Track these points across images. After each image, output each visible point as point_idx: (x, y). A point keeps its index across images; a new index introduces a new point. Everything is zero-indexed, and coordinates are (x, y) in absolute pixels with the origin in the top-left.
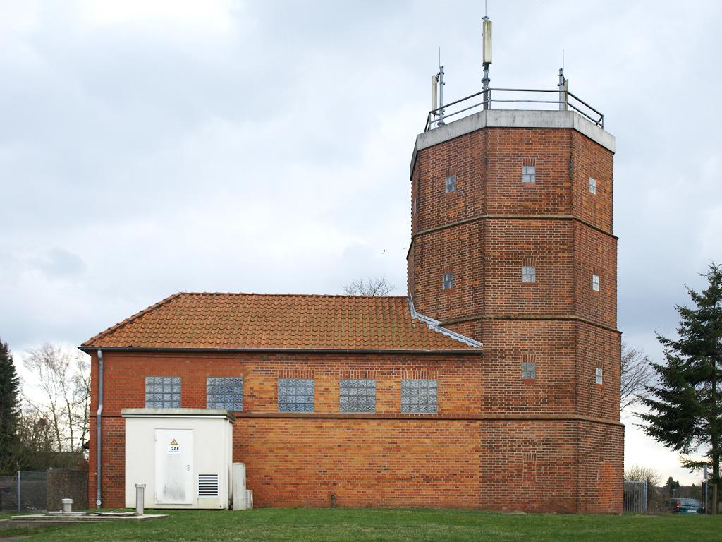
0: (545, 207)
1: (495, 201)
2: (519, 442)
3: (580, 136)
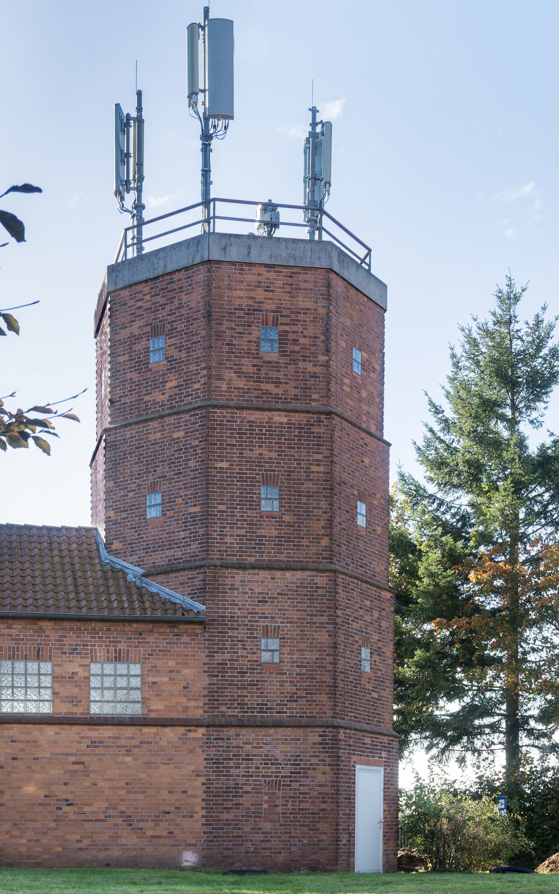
0: (293, 392)
1: (223, 379)
2: (257, 761)
3: (340, 283)
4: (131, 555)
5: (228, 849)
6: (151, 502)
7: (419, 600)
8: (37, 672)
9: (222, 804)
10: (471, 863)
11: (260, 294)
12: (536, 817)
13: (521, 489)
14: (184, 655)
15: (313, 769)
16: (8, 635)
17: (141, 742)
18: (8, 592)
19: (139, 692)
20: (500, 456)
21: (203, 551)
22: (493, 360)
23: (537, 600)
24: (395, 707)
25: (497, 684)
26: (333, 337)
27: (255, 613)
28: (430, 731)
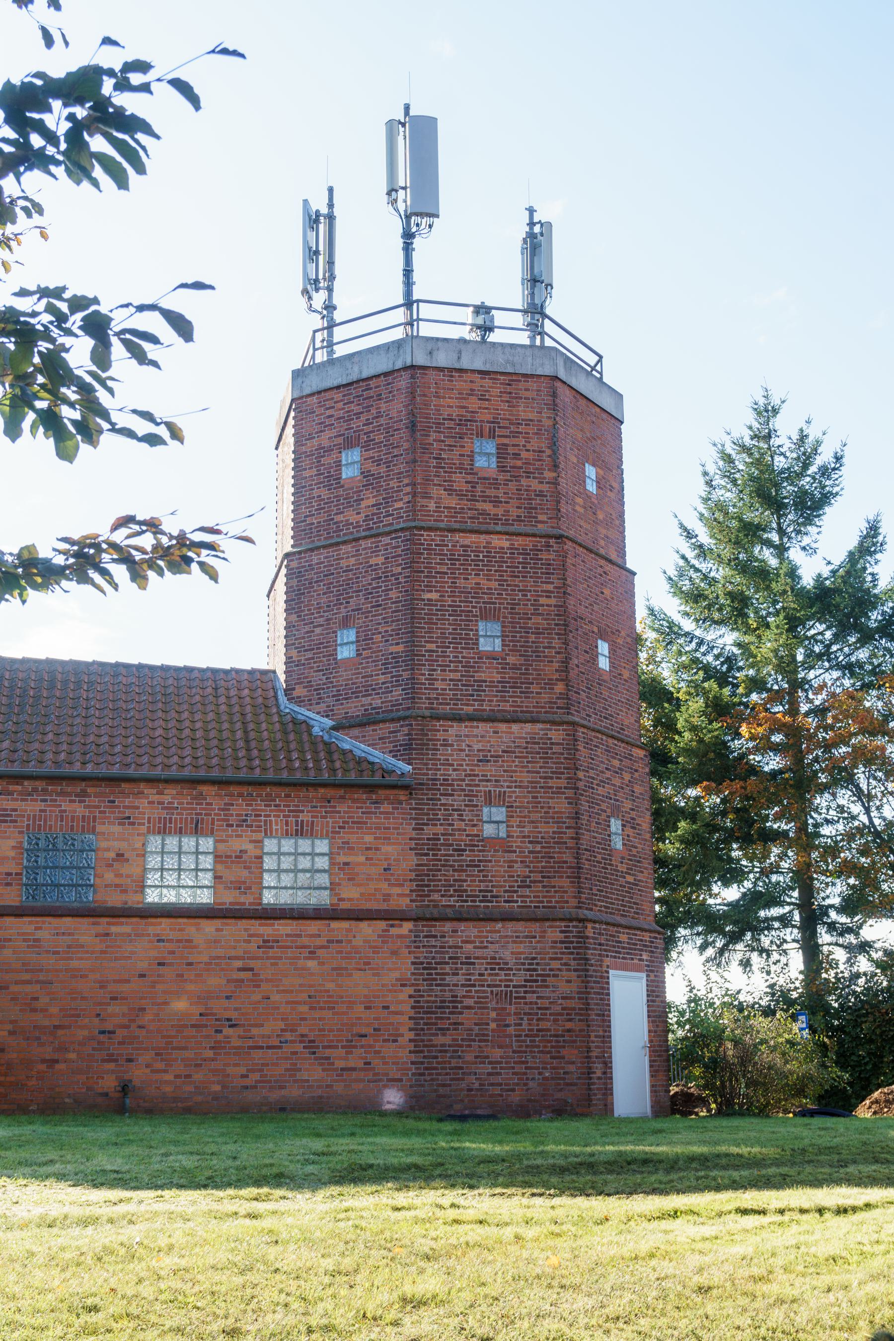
0: (514, 512)
1: (431, 498)
2: (481, 966)
3: (568, 392)
4: (318, 703)
5: (444, 1085)
6: (342, 639)
7: (680, 760)
8: (194, 850)
9: (436, 1024)
10: (768, 1103)
11: (473, 403)
12: (848, 1039)
13: (797, 627)
14: (385, 828)
15: (554, 976)
16: (159, 803)
17: (328, 941)
18: (160, 748)
19: (326, 876)
20: (768, 588)
21: (408, 699)
22: (752, 479)
23: (826, 759)
24: (657, 894)
25: (785, 865)
26: (561, 451)
27: (474, 775)
28: (704, 925)
